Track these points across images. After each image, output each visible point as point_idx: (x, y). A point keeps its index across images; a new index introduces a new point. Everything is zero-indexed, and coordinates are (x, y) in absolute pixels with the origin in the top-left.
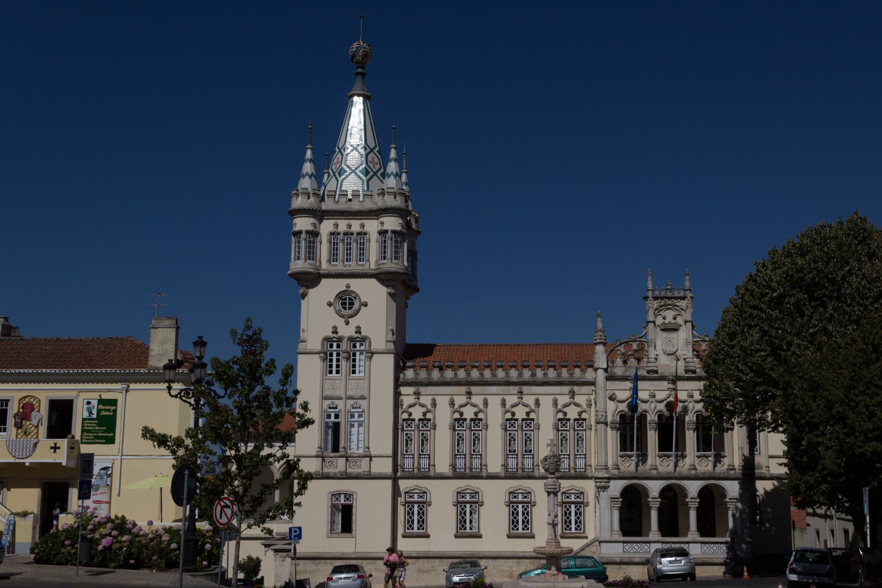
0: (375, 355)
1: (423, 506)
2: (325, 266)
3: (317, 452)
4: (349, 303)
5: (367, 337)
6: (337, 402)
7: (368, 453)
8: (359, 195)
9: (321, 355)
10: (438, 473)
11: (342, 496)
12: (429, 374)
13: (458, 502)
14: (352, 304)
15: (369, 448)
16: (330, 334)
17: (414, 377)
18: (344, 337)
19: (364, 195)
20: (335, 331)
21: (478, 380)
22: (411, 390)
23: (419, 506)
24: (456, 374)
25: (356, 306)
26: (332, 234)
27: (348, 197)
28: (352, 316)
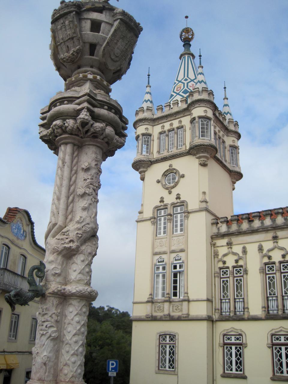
0: (191, 216)
1: (240, 348)
2: (156, 156)
3: (148, 298)
4: (172, 178)
5: (185, 201)
6: (164, 256)
7: (186, 298)
8: (178, 103)
9: (152, 220)
10: (252, 316)
11: (168, 337)
12: (240, 226)
13: (273, 345)
14: (174, 179)
15: (187, 293)
16: (159, 204)
17: (226, 230)
18: (168, 204)
19: (181, 101)
20: (162, 201)
21: (282, 225)
22: (224, 241)
23: (236, 348)
24: (262, 223)
25: (176, 180)
26: (161, 133)
27: (171, 107)
28: (173, 187)
